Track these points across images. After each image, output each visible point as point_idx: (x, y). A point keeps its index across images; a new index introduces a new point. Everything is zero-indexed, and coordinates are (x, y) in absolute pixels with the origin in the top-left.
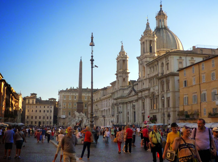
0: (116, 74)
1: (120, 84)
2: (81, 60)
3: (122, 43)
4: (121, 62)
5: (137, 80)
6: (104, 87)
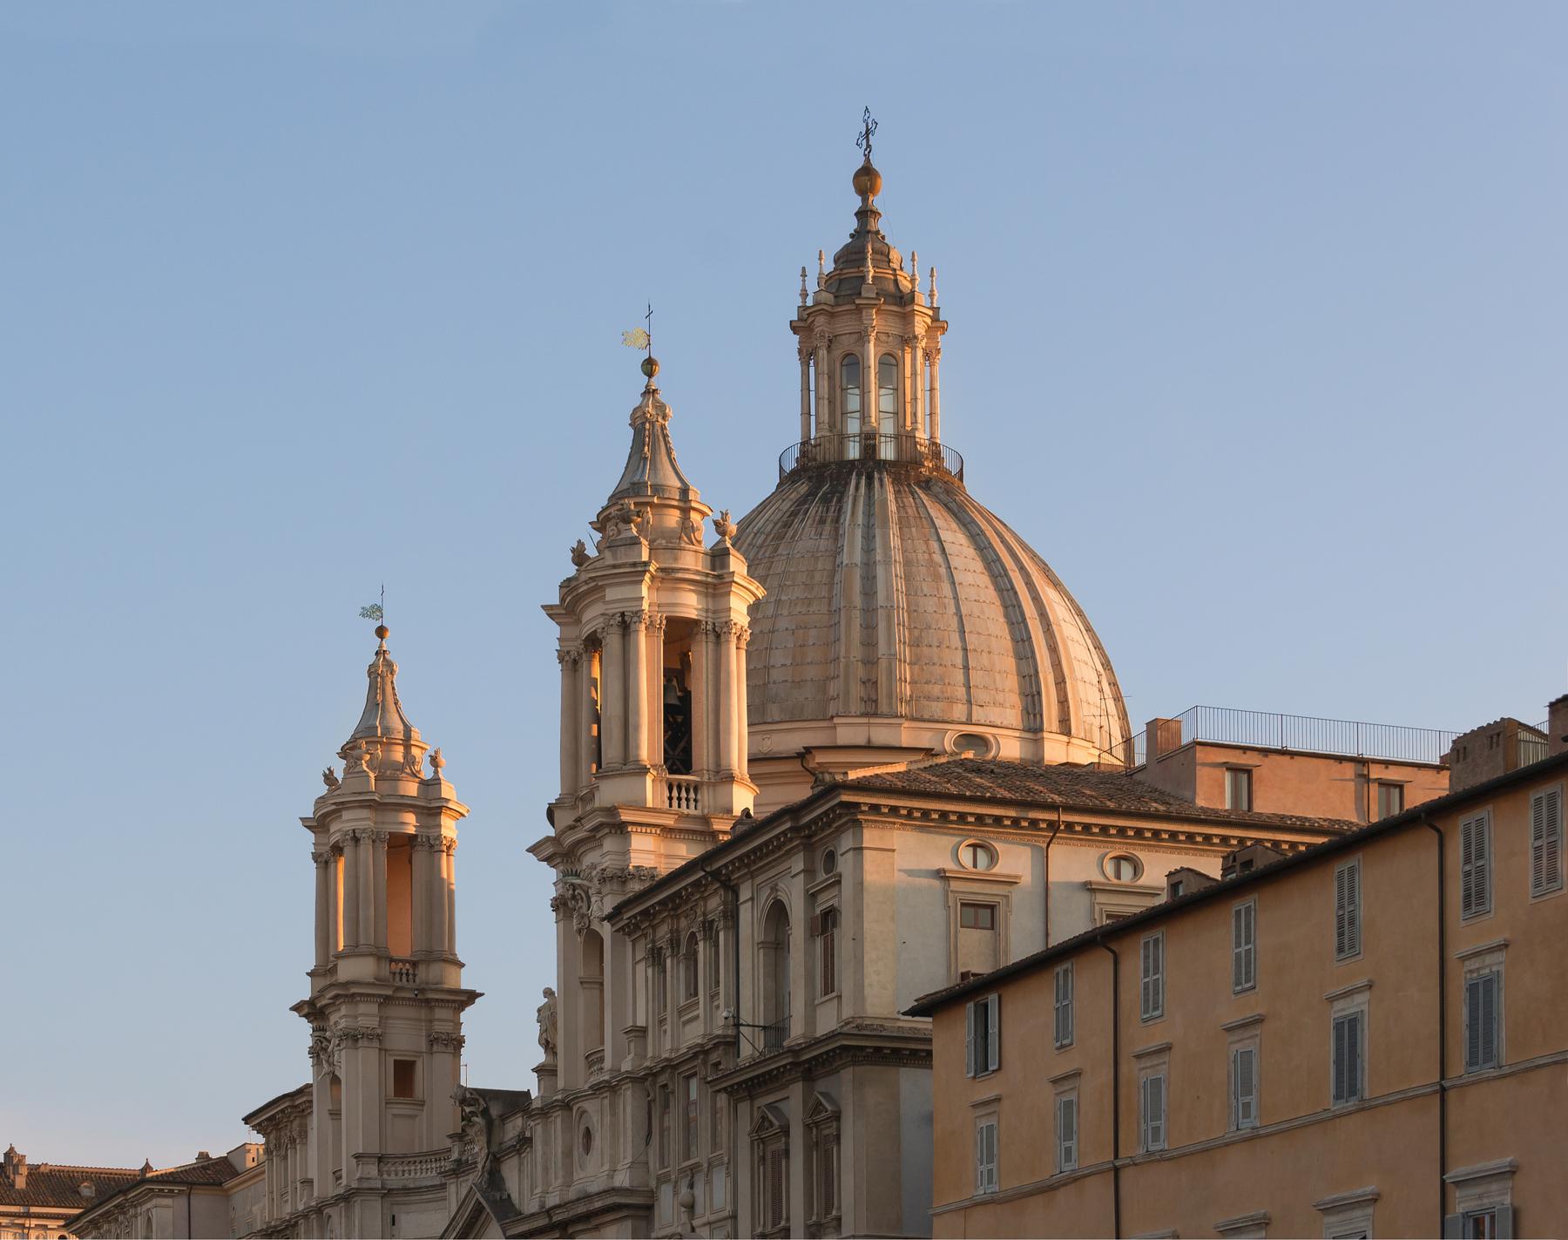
0: (312, 1010)
1: (357, 1132)
5: (529, 1083)
6: (203, 1156)
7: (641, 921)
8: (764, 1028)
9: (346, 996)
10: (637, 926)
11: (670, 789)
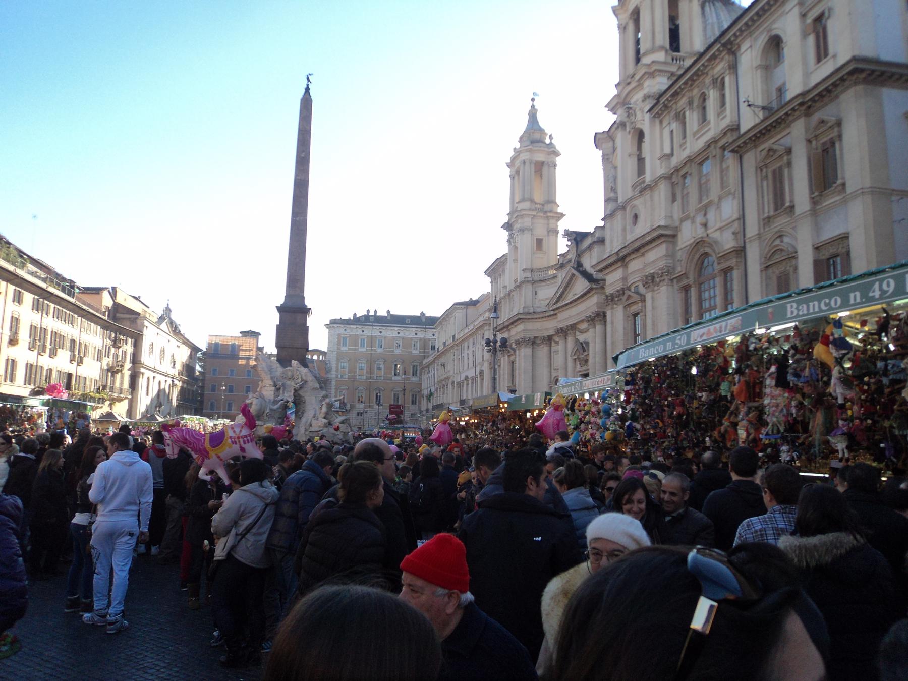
0: (508, 226)
2: (307, 89)
3: (533, 100)
4: (528, 170)
6: (471, 299)
7: (671, 101)
8: (763, 108)
9: (521, 216)
10: (666, 107)
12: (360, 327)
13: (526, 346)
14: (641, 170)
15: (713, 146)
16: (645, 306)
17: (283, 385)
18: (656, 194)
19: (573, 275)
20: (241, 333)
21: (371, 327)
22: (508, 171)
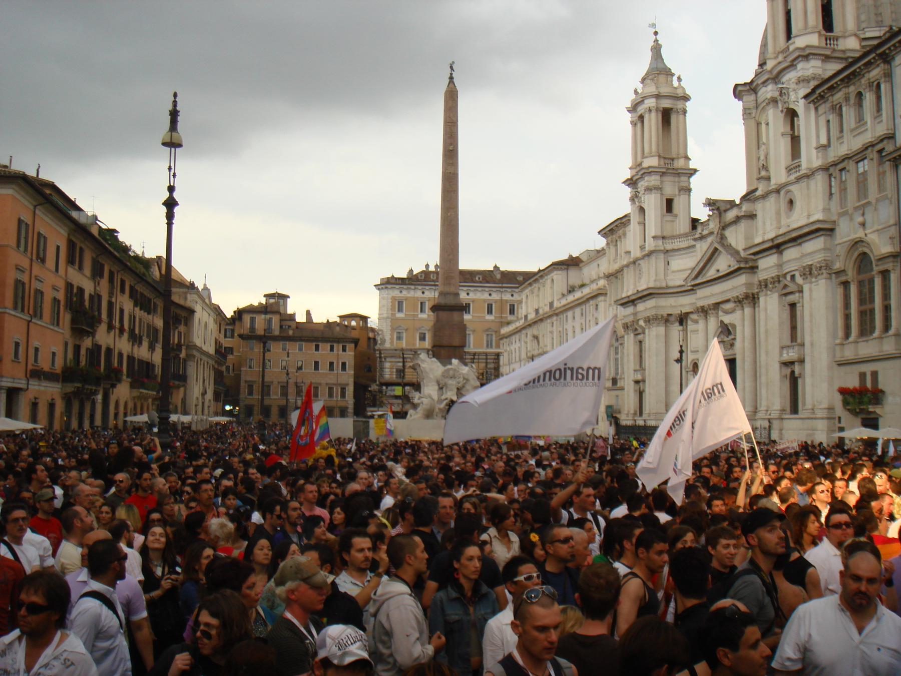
0: (631, 183)
2: (451, 78)
3: (656, 33)
6: (571, 256)
10: (822, 97)
11: (826, 40)
12: (420, 287)
13: (658, 325)
14: (795, 151)
15: (870, 149)
16: (803, 297)
17: (446, 385)
18: (812, 183)
19: (716, 249)
20: (265, 296)
21: (434, 288)
22: (628, 117)
